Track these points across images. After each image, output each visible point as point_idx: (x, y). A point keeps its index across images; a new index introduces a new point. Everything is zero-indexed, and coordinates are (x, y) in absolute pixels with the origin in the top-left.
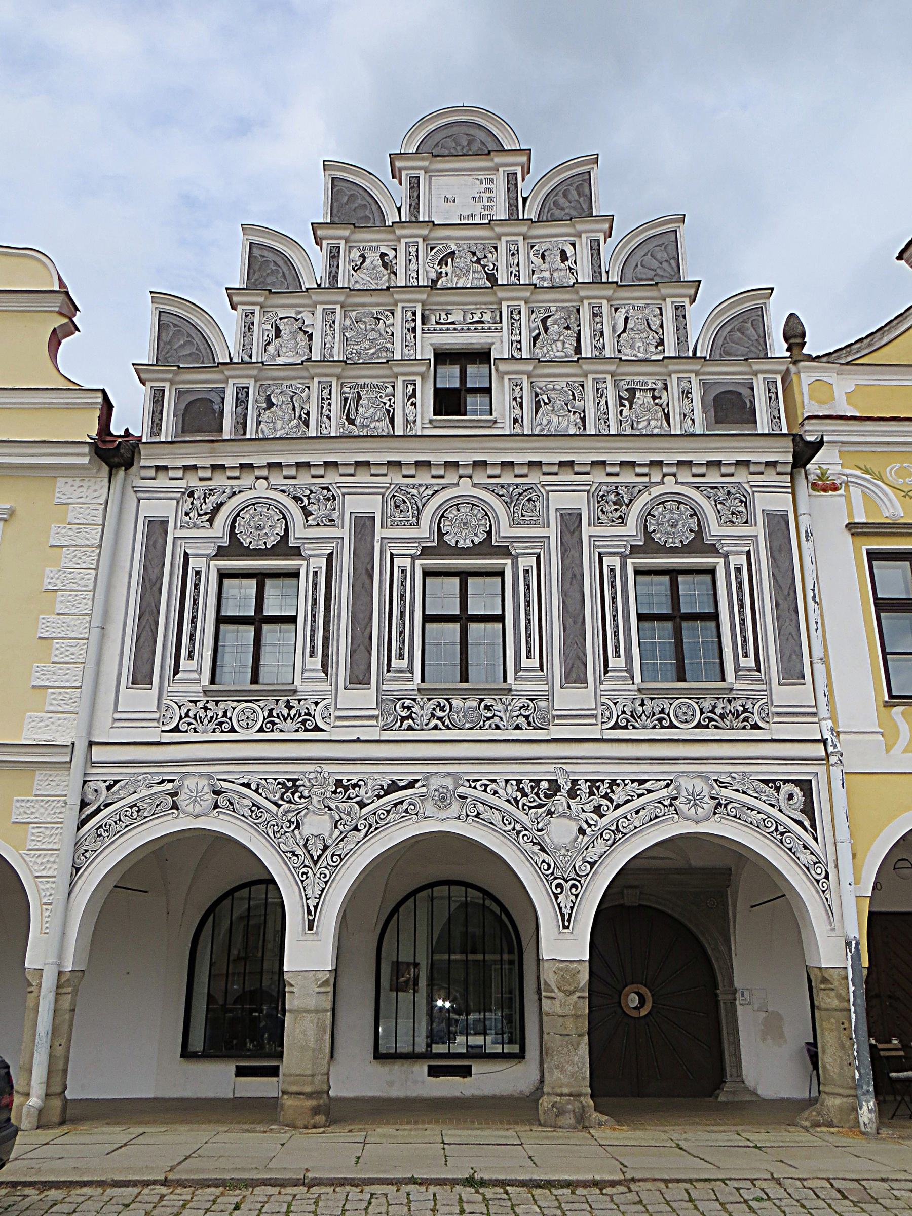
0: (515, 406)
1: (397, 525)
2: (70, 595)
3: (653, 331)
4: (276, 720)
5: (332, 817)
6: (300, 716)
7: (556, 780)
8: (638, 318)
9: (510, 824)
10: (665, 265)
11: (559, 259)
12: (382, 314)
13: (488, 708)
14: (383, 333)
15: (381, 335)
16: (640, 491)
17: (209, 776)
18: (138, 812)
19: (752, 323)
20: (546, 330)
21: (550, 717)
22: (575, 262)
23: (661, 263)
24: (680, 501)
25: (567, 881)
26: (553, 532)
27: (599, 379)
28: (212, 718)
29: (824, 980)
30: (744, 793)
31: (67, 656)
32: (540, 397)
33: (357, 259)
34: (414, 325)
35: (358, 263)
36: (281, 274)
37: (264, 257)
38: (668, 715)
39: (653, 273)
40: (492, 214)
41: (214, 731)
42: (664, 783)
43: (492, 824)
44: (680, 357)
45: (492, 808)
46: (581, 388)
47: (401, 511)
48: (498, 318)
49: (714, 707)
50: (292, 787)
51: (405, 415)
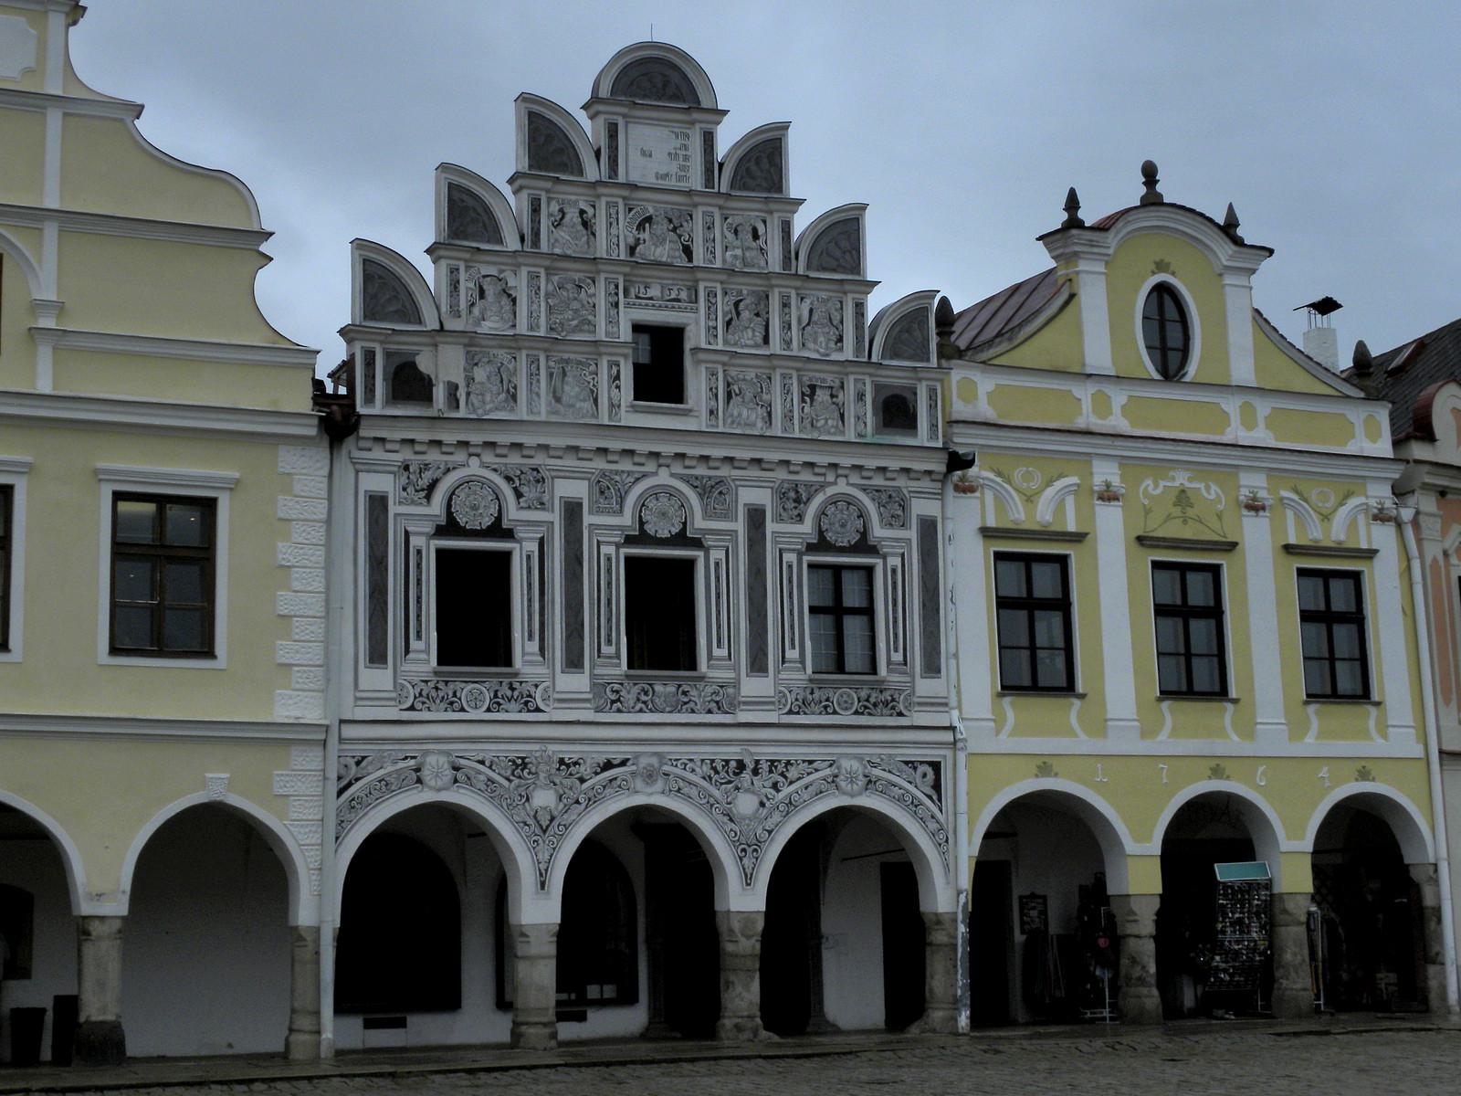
1: (602, 512)
2: (304, 572)
4: (501, 701)
5: (557, 791)
6: (522, 698)
7: (742, 760)
9: (705, 798)
10: (848, 256)
11: (750, 236)
12: (584, 281)
13: (685, 693)
14: (585, 303)
15: (583, 305)
16: (816, 490)
17: (448, 753)
18: (387, 785)
19: (919, 324)
20: (738, 314)
21: (736, 702)
24: (849, 501)
25: (749, 846)
26: (740, 526)
28: (443, 698)
29: (939, 922)
30: (890, 772)
31: (307, 634)
32: (731, 387)
33: (556, 213)
35: (558, 218)
36: (481, 224)
37: (463, 201)
38: (833, 703)
39: (836, 263)
41: (446, 710)
42: (828, 763)
43: (690, 797)
45: (690, 784)
47: (606, 498)
48: (694, 297)
49: (869, 696)
50: (521, 764)
51: (610, 399)
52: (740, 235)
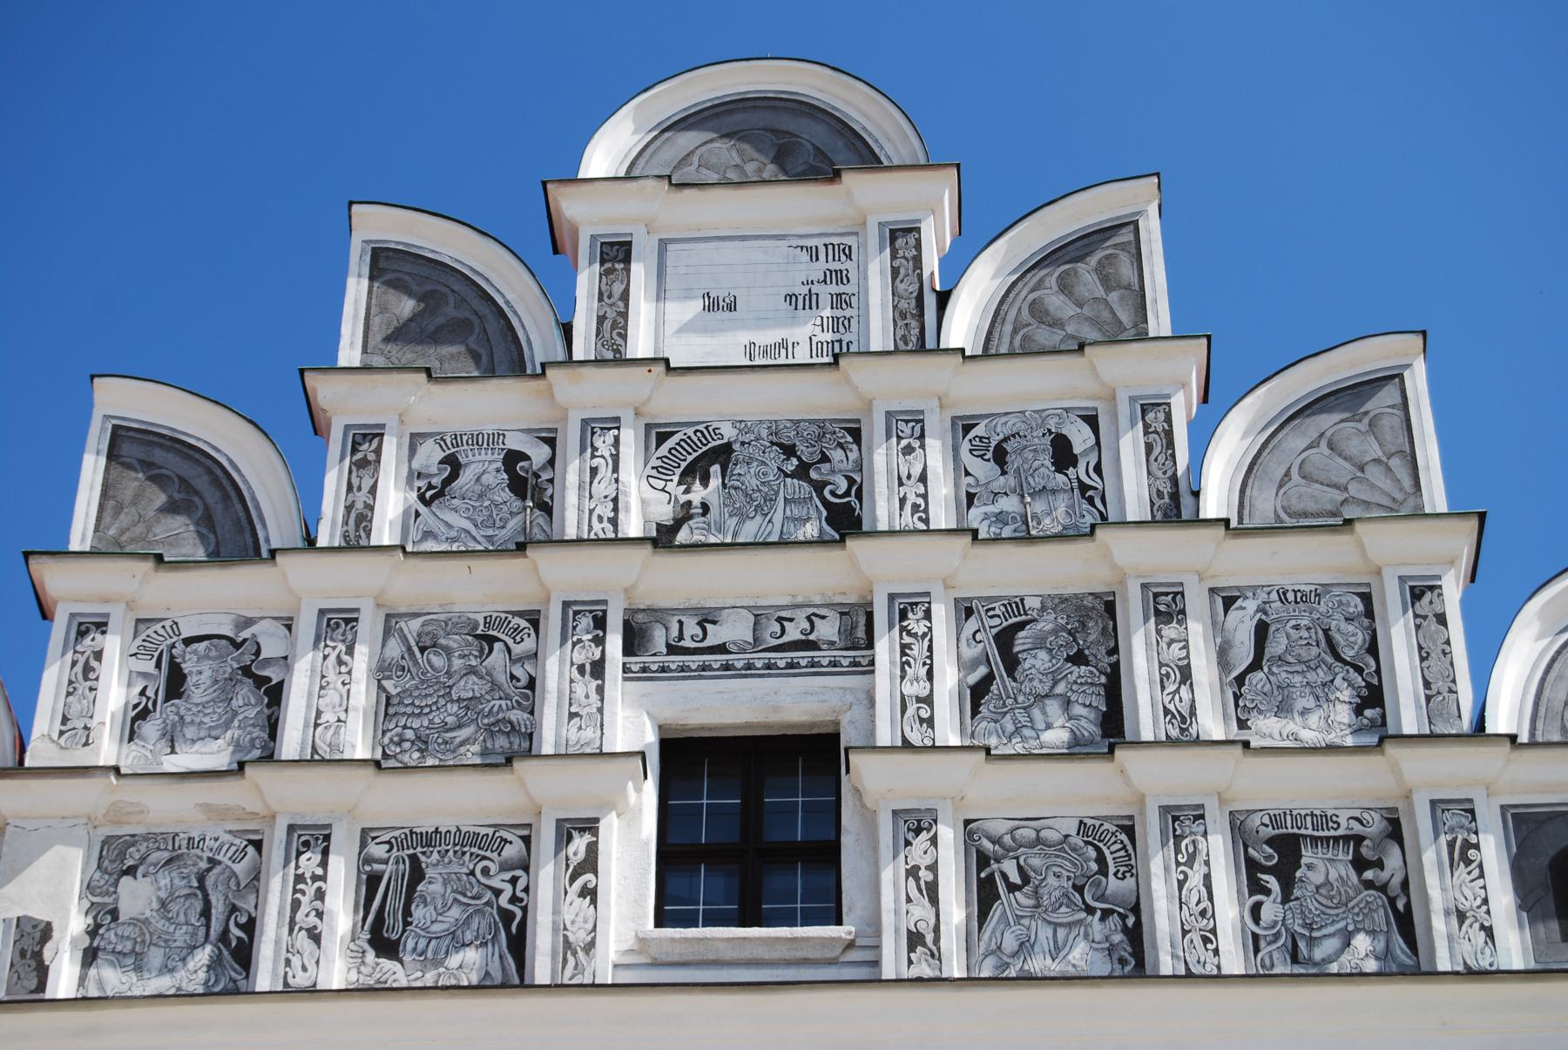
0: (914, 893)
3: (1345, 663)
8: (1297, 627)
10: (1374, 473)
14: (502, 678)
15: (495, 686)
20: (1012, 663)
22: (1098, 469)
23: (1363, 471)
27: (1179, 808)
32: (995, 866)
33: (434, 470)
34: (598, 655)
35: (436, 481)
40: (846, 338)
44: (1433, 736)
46: (1123, 837)
48: (861, 633)
51: (559, 928)
52: (1014, 462)
